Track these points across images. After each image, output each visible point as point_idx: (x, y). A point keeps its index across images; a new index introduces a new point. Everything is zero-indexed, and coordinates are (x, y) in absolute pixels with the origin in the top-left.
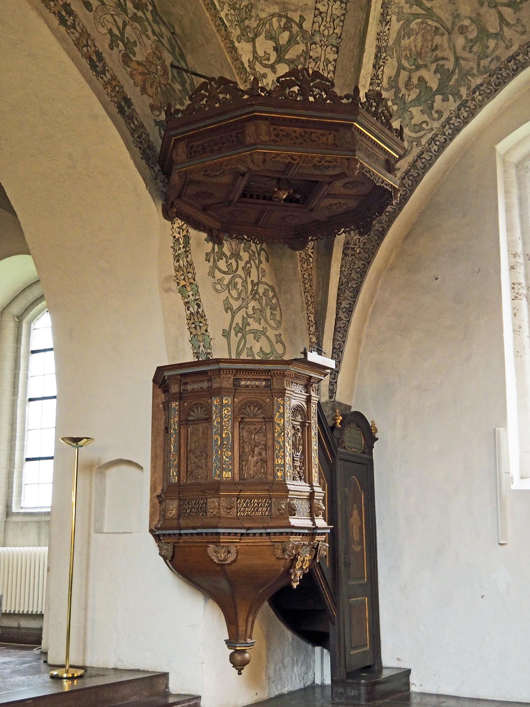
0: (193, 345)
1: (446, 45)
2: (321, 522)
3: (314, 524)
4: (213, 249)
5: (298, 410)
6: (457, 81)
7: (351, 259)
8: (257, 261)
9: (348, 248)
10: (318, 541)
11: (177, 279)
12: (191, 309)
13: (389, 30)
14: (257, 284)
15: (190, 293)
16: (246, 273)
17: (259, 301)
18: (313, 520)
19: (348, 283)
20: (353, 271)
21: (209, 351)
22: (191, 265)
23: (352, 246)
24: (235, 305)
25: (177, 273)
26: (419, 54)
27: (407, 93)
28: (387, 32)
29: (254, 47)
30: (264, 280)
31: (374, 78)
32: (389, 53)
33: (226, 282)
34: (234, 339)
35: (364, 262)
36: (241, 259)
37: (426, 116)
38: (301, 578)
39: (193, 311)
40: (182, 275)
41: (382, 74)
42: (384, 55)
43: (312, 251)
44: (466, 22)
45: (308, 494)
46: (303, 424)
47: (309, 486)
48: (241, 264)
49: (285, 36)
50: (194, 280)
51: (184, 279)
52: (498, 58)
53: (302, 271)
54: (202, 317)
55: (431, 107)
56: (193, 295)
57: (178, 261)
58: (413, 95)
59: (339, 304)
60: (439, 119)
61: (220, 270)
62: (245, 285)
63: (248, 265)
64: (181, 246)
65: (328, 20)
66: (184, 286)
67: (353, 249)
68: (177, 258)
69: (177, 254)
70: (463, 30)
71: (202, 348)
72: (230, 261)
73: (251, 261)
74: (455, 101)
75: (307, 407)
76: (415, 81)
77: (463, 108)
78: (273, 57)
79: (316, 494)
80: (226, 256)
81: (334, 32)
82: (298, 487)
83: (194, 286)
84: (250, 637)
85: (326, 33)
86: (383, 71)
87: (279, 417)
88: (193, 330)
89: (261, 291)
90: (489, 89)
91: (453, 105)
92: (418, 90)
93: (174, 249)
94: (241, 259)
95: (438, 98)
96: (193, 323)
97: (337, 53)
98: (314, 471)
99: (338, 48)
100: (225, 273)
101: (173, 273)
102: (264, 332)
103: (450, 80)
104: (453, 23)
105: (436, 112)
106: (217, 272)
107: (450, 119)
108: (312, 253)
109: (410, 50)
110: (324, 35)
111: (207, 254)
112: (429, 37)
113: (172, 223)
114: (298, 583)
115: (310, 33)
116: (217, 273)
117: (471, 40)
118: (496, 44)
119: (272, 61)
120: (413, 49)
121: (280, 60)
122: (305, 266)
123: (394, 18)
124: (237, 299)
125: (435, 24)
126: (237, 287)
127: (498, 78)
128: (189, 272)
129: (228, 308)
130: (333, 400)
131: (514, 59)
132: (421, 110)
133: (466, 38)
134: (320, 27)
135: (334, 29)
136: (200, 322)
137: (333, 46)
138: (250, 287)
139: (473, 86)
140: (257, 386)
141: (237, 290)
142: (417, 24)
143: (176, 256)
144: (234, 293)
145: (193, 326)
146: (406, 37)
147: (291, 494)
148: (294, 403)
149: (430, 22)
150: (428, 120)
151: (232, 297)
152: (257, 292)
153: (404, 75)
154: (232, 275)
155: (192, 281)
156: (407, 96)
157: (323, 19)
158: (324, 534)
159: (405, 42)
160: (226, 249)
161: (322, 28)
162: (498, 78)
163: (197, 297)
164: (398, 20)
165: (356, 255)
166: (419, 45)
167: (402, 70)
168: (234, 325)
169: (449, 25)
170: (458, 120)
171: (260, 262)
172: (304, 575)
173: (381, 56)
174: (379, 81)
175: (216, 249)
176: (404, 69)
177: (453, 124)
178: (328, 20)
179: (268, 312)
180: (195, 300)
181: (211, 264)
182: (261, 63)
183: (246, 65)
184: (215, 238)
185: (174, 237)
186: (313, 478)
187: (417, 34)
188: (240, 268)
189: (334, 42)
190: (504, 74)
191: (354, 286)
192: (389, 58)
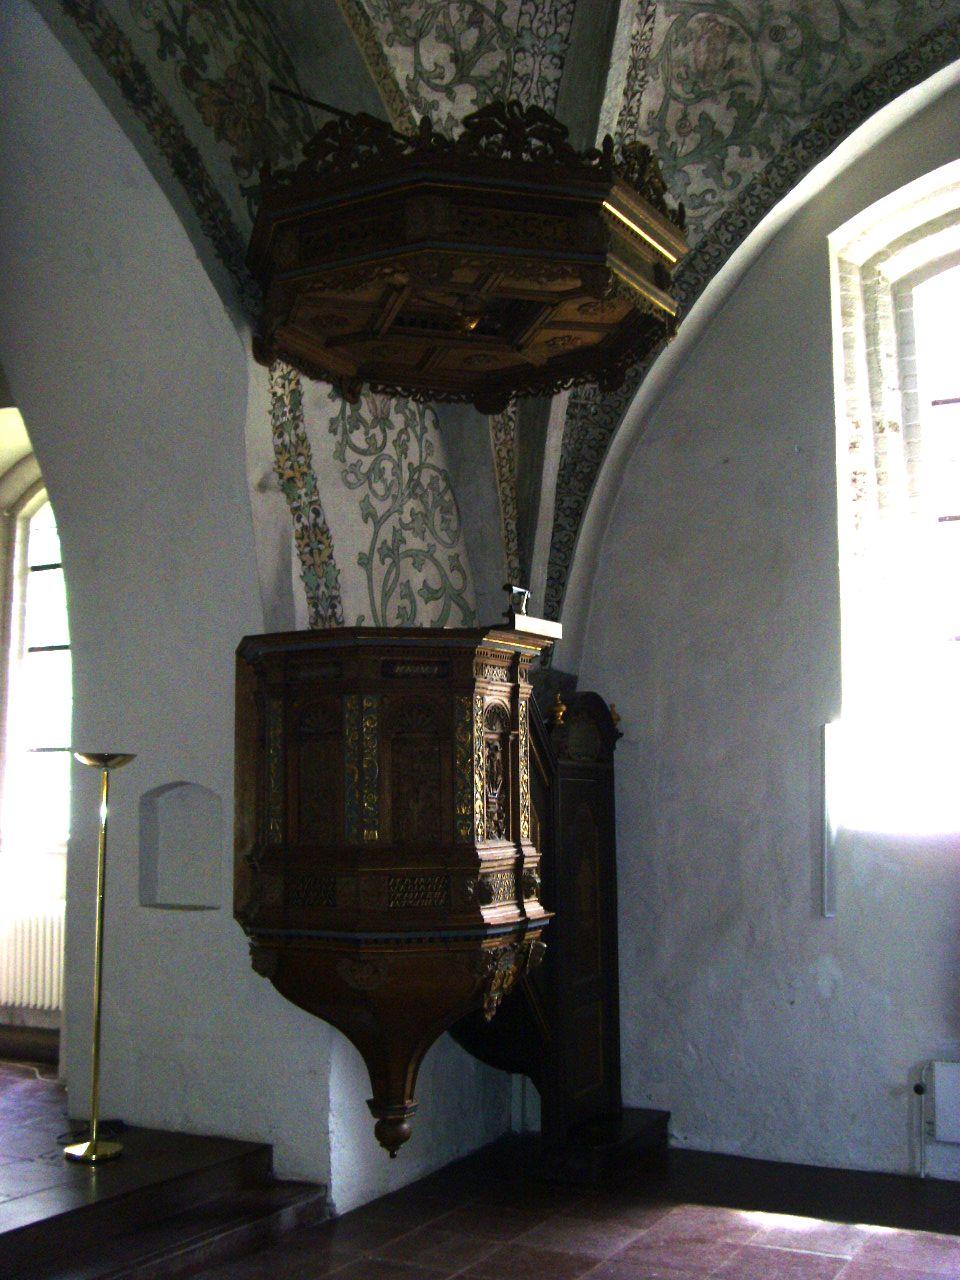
0: (306, 584)
1: (747, 61)
2: (534, 908)
3: (523, 913)
4: (343, 410)
5: (495, 714)
6: (766, 122)
7: (580, 424)
8: (418, 429)
9: (576, 405)
10: (529, 940)
11: (279, 467)
12: (304, 519)
13: (651, 29)
14: (419, 469)
15: (302, 492)
16: (399, 450)
17: (421, 498)
18: (520, 906)
19: (575, 464)
20: (585, 446)
21: (335, 593)
22: (303, 441)
23: (583, 402)
24: (381, 508)
25: (279, 457)
26: (702, 74)
27: (680, 140)
28: (649, 34)
29: (417, 55)
30: (430, 460)
31: (624, 113)
32: (651, 69)
33: (364, 469)
34: (379, 569)
35: (602, 430)
36: (391, 427)
37: (711, 180)
38: (499, 1002)
39: (306, 523)
40: (289, 459)
41: (638, 107)
42: (642, 73)
43: (514, 409)
44: (784, 21)
45: (512, 861)
46: (503, 738)
47: (514, 847)
48: (392, 435)
49: (470, 37)
50: (309, 466)
51: (292, 467)
52: (836, 86)
53: (496, 445)
54: (322, 533)
55: (721, 168)
56: (306, 494)
57: (281, 435)
58: (690, 144)
59: (559, 500)
60: (732, 187)
61: (355, 449)
62: (398, 472)
63: (404, 437)
64: (286, 409)
65: (547, 10)
66: (291, 480)
67: (584, 407)
68: (279, 431)
69: (278, 423)
70: (777, 35)
71: (323, 588)
72: (372, 432)
73: (409, 429)
74: (762, 158)
75: (512, 706)
76: (694, 120)
77: (774, 170)
78: (450, 73)
79: (526, 860)
81: (555, 32)
82: (495, 853)
83: (308, 478)
84: (411, 1097)
85: (542, 31)
86: (639, 100)
87: (462, 730)
88: (307, 557)
89: (425, 480)
90: (820, 139)
91: (757, 164)
92: (698, 136)
94: (391, 427)
95: (734, 150)
96: (307, 545)
97: (561, 67)
98: (522, 818)
99: (561, 58)
100: (363, 453)
102: (429, 554)
103: (754, 121)
104: (762, 21)
105: (730, 174)
106: (349, 452)
107: (752, 187)
108: (514, 412)
109: (687, 66)
110: (539, 37)
112: (720, 46)
113: (270, 371)
114: (494, 1013)
115: (515, 31)
116: (349, 453)
117: (791, 53)
118: (834, 62)
119: (446, 81)
120: (692, 66)
121: (462, 77)
122: (502, 435)
123: (661, 9)
124: (384, 498)
125: (728, 22)
126: (385, 476)
127: (835, 121)
128: (300, 454)
129: (368, 514)
130: (547, 667)
131: (865, 88)
132: (703, 171)
133: (782, 49)
134: (532, 22)
135: (557, 26)
136: (320, 542)
137: (555, 56)
138: (406, 475)
139: (793, 133)
140: (424, 676)
141: (384, 481)
142: (699, 20)
144: (379, 487)
145: (307, 549)
146: (681, 44)
147: (484, 868)
148: (489, 700)
149: (721, 19)
150: (715, 187)
152: (418, 484)
153: (675, 108)
154: (374, 457)
155: (305, 469)
156: (679, 146)
157: (537, 7)
158: (540, 927)
159: (680, 52)
160: (365, 412)
161: (536, 24)
162: (835, 121)
163: (314, 498)
164: (668, 14)
165: (590, 417)
166: (702, 58)
167: (672, 102)
169: (754, 25)
170: (767, 190)
171: (424, 429)
172: (504, 998)
173: (637, 75)
174: (632, 118)
175: (348, 411)
176: (676, 98)
177: (758, 197)
178: (547, 10)
179: (437, 517)
180: (311, 503)
181: (339, 437)
182: (428, 83)
183: (403, 86)
184: (347, 390)
185: (274, 394)
186: (522, 830)
187: (699, 40)
188: (389, 444)
189: (556, 48)
190: (847, 115)
191: (586, 470)
192: (650, 79)
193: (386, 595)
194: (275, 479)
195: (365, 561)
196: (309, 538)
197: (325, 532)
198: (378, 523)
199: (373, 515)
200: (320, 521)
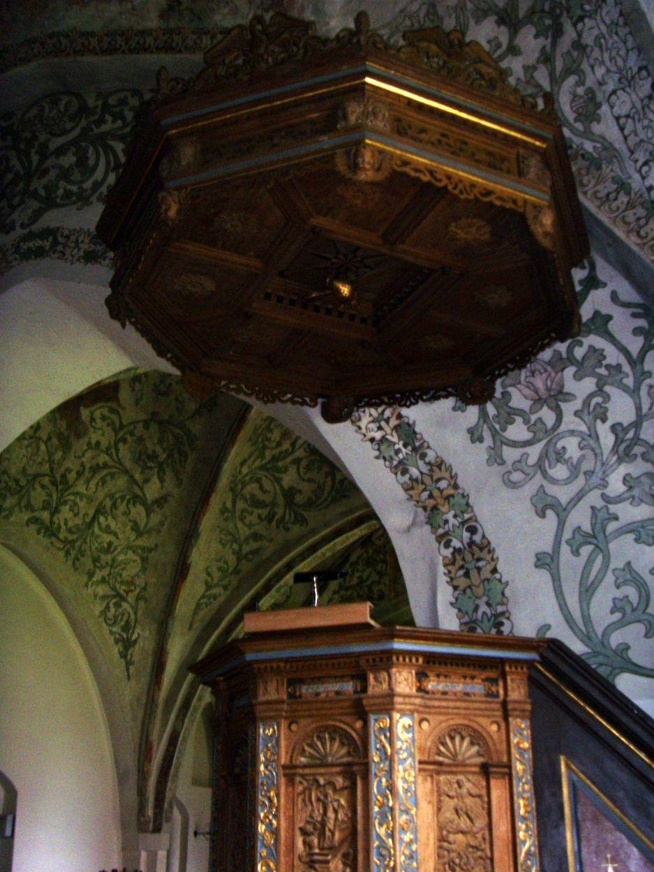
0: (460, 610)
4: (483, 415)
15: (450, 516)
21: (500, 609)
22: (439, 467)
24: (563, 494)
40: (424, 490)
51: (431, 496)
54: (481, 549)
56: (455, 516)
57: (405, 472)
61: (514, 444)
64: (400, 445)
66: (435, 508)
69: (395, 463)
71: (483, 608)
72: (533, 418)
78: (503, 35)
80: (521, 413)
83: (458, 499)
88: (463, 582)
93: (384, 458)
94: (569, 397)
96: (462, 567)
101: (402, 494)
111: (471, 431)
113: (353, 422)
116: (510, 454)
119: (504, 40)
124: (568, 481)
128: (439, 480)
129: (543, 505)
136: (479, 560)
143: (396, 467)
144: (560, 472)
145: (461, 572)
151: (554, 481)
155: (451, 491)
160: (519, 400)
163: (467, 516)
168: (567, 535)
180: (463, 523)
181: (488, 441)
185: (372, 440)
193: (587, 591)
194: (422, 516)
195: (547, 561)
196: (463, 559)
197: (486, 546)
198: (562, 512)
199: (554, 505)
200: (477, 538)
